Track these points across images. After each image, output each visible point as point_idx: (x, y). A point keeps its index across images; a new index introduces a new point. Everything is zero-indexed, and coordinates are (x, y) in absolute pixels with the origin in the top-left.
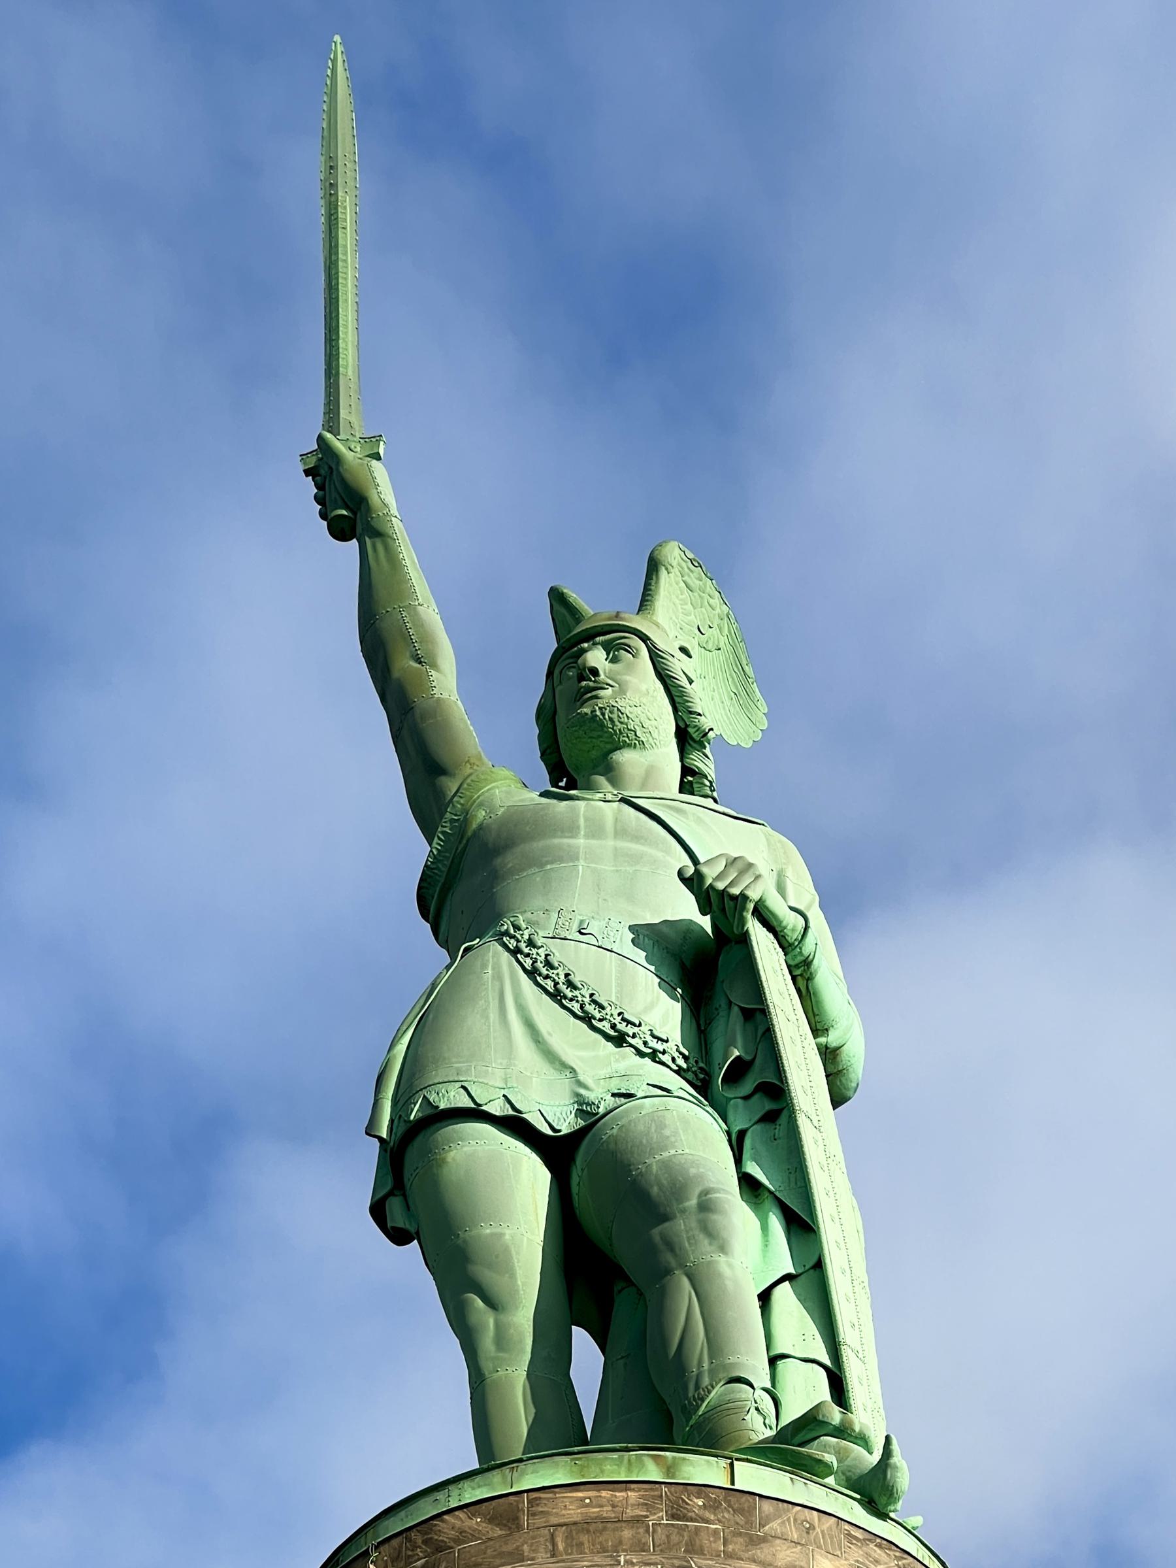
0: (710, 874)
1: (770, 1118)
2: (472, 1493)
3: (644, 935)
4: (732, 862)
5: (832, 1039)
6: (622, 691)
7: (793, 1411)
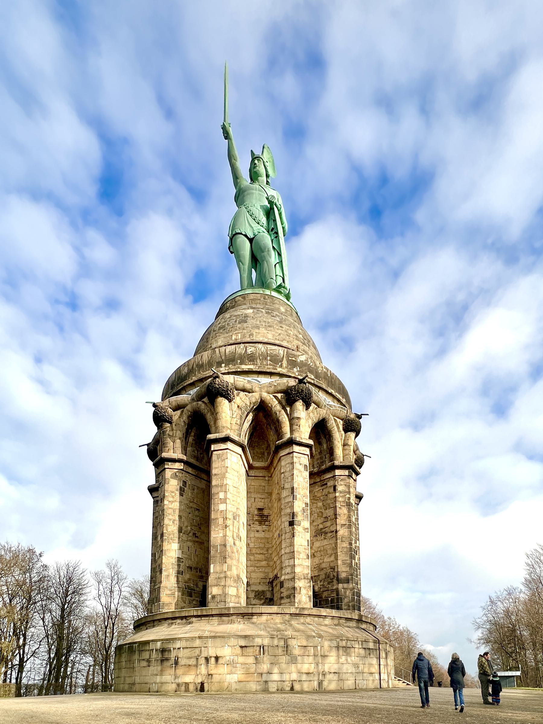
0: (270, 198)
1: (276, 237)
2: (240, 293)
3: (262, 207)
4: (273, 196)
5: (284, 225)
6: (259, 168)
7: (278, 284)
